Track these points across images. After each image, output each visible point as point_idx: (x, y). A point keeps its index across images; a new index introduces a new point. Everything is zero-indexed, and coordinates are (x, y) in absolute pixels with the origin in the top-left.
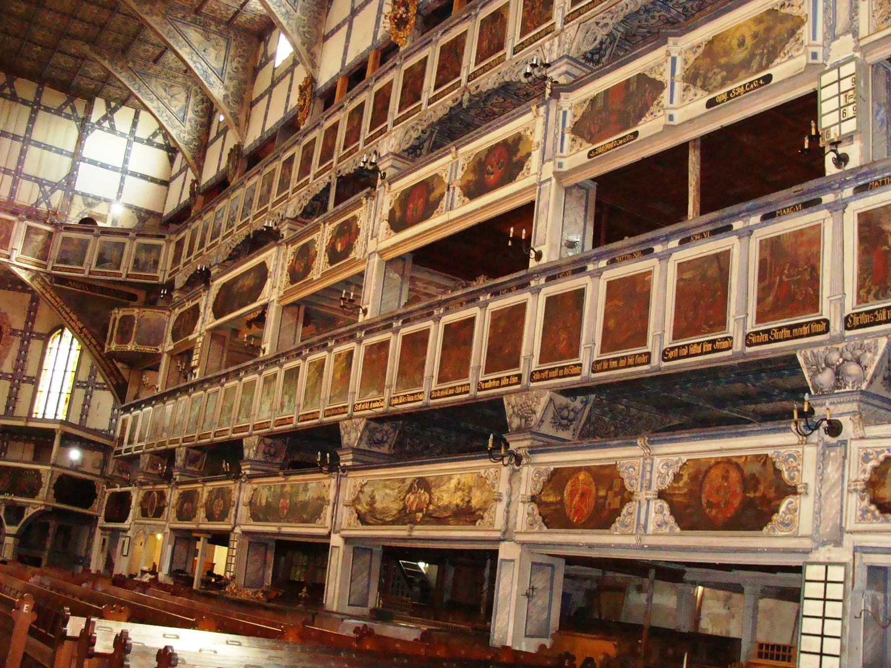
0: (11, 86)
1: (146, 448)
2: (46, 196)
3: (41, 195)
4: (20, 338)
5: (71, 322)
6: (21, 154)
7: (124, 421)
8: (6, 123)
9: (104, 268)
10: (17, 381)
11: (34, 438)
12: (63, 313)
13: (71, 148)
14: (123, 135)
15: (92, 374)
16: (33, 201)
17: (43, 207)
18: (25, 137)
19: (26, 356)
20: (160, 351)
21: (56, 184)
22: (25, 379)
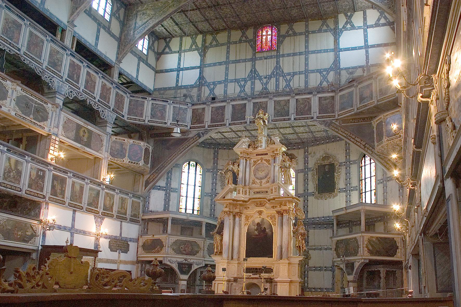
0: (292, 29)
2: (325, 78)
3: (322, 78)
6: (306, 61)
8: (294, 49)
9: (364, 103)
10: (348, 191)
13: (332, 47)
14: (359, 28)
16: (319, 82)
17: (325, 84)
18: (305, 52)
21: (329, 69)
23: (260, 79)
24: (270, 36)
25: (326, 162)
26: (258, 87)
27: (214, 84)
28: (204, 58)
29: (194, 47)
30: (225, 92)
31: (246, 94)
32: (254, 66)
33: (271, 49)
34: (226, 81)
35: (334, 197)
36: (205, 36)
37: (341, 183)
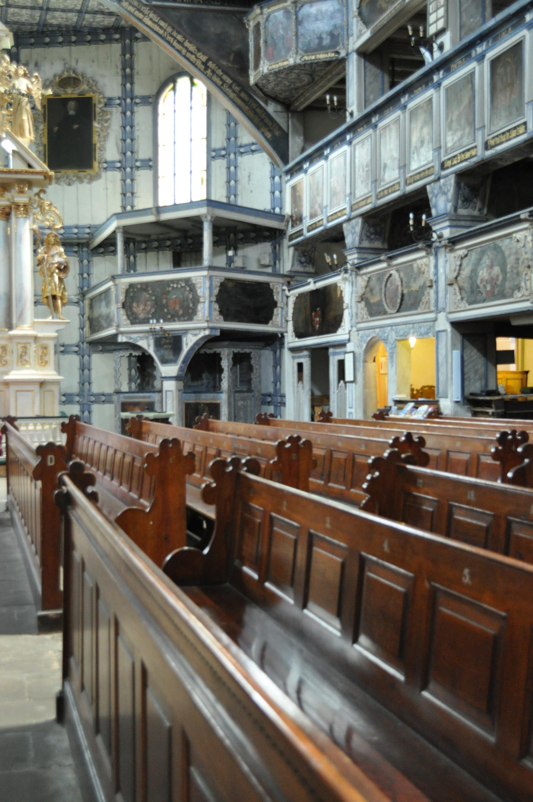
1: (352, 210)
4: (120, 109)
5: (188, 55)
7: (294, 189)
10: (128, 170)
11: (168, 243)
12: (175, 44)
15: (232, 134)
19: (132, 133)
20: (343, 54)
22: (138, 164)
25: (70, 92)
35: (92, 179)
37: (109, 149)
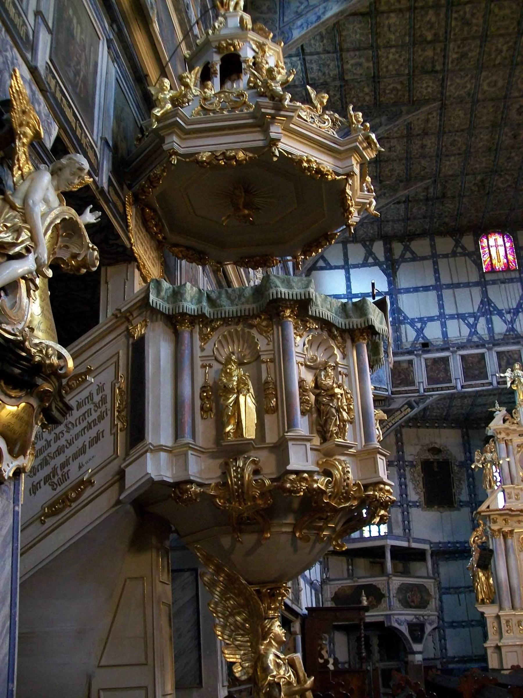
23: (500, 313)
24: (503, 248)
26: (500, 327)
27: (421, 320)
28: (394, 279)
29: (371, 260)
30: (445, 334)
31: (480, 338)
32: (485, 294)
33: (507, 268)
34: (442, 317)
36: (390, 244)
